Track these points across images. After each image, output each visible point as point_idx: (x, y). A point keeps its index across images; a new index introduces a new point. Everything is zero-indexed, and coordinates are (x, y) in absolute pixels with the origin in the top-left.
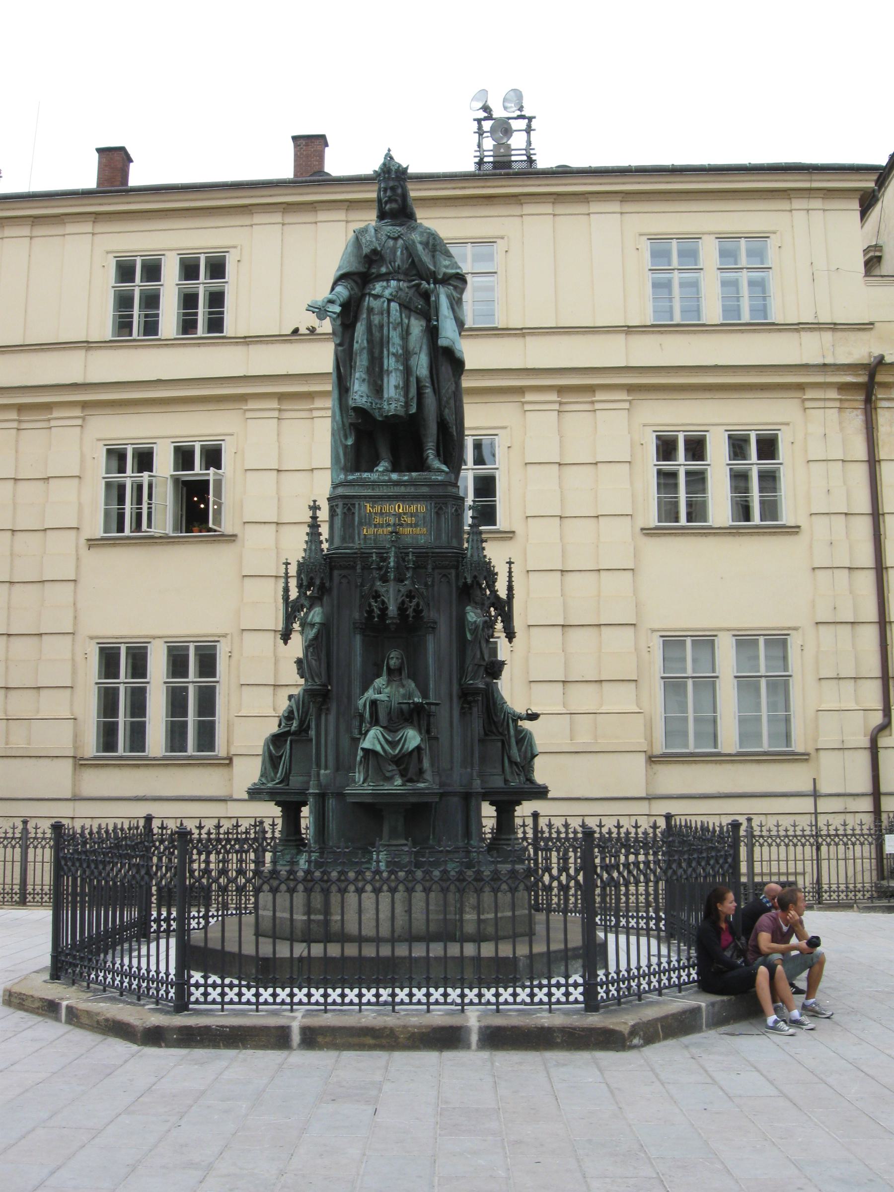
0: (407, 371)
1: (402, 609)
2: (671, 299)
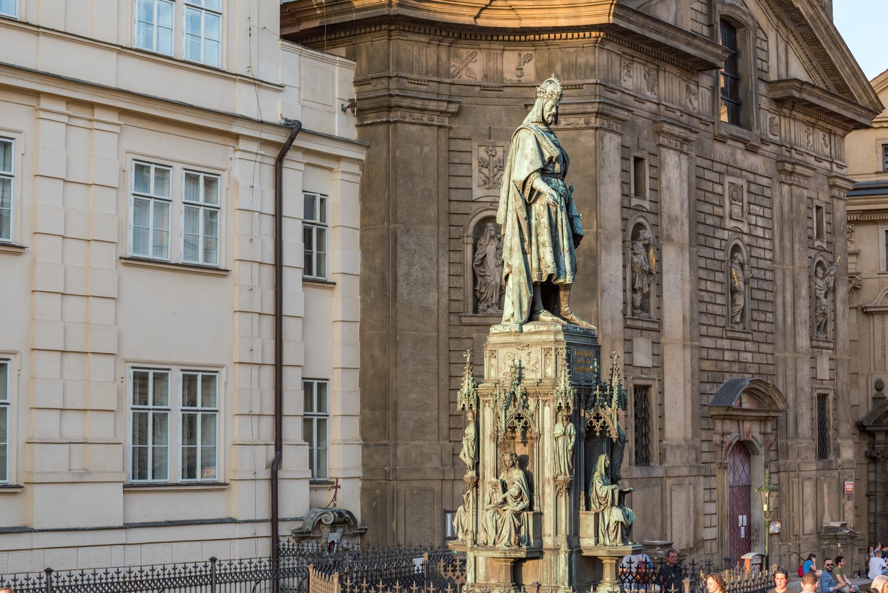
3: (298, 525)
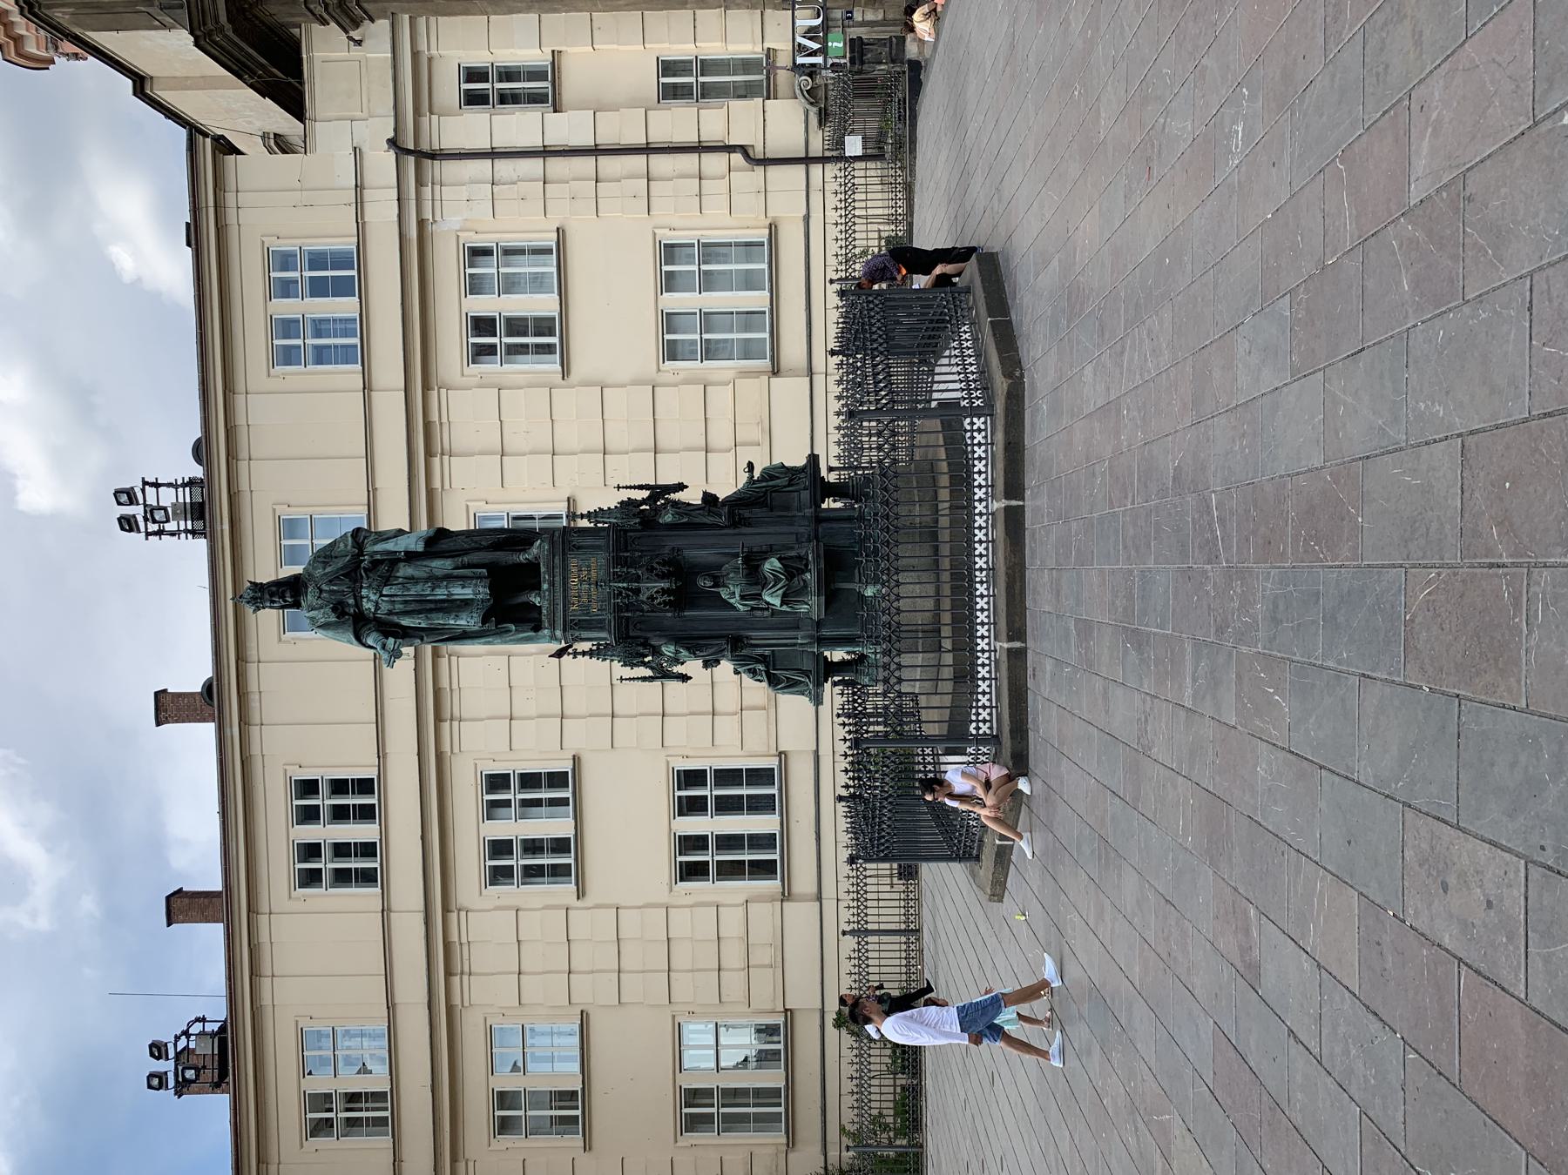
0: (449, 578)
1: (662, 577)
2: (336, 347)
3: (814, 120)
